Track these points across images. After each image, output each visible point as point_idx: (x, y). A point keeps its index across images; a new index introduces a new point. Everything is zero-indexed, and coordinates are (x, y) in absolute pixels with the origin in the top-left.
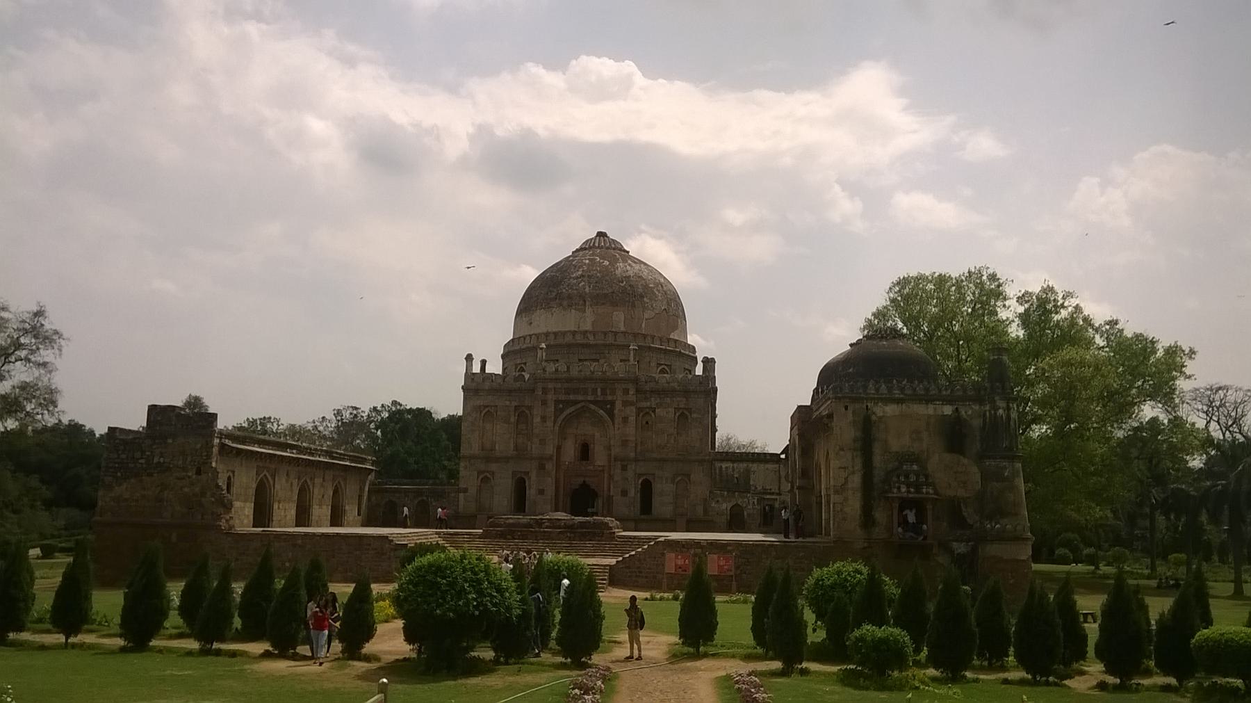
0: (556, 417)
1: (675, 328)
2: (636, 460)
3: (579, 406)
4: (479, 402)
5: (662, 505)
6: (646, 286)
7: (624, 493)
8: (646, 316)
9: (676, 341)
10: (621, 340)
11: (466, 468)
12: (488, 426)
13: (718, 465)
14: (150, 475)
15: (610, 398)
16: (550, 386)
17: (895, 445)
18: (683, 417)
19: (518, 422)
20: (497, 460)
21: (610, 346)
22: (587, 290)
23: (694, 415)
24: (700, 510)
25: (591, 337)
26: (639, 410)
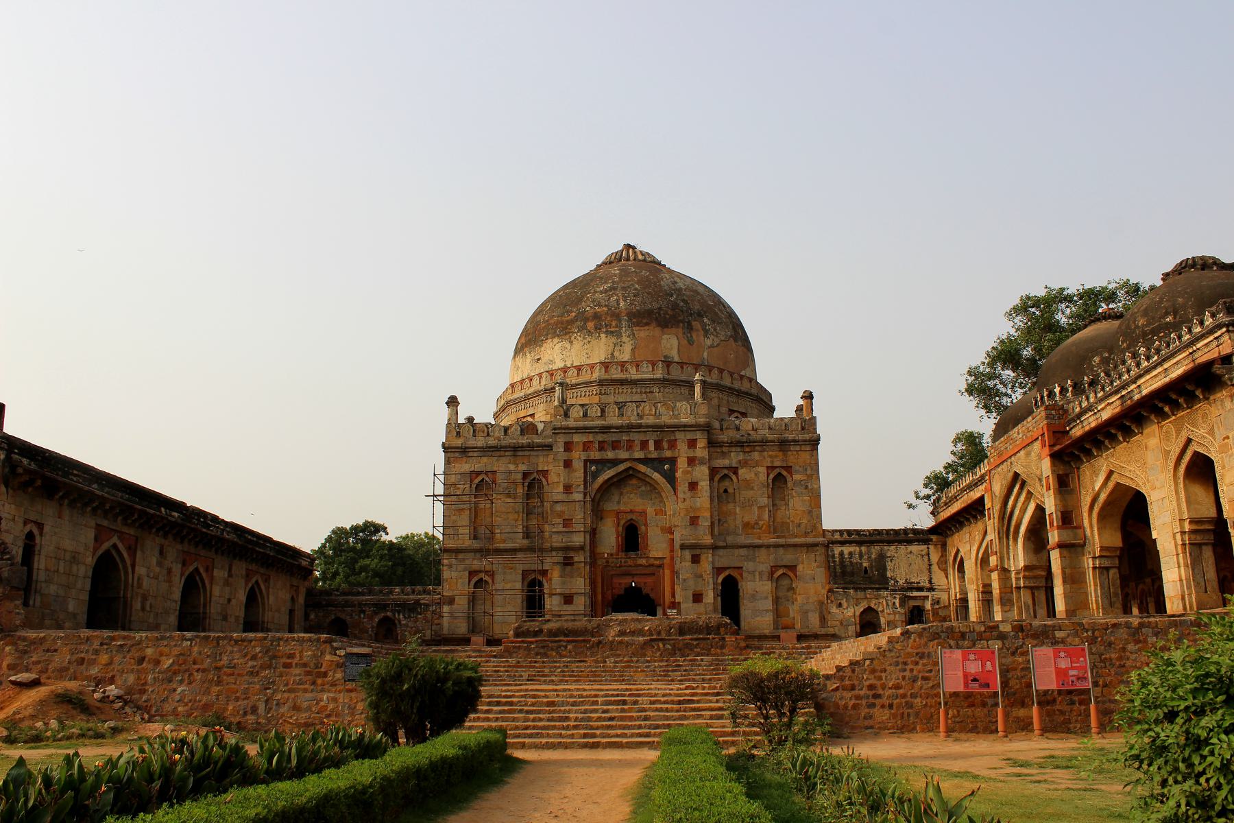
2: (715, 548)
3: (622, 467)
4: (466, 467)
5: (757, 613)
7: (697, 598)
8: (708, 342)
9: (752, 380)
11: (450, 566)
12: (483, 504)
13: (837, 550)
15: (668, 454)
16: (577, 438)
18: (779, 481)
19: (528, 496)
22: (622, 304)
23: (797, 477)
24: (814, 620)
25: (633, 371)
26: (713, 471)
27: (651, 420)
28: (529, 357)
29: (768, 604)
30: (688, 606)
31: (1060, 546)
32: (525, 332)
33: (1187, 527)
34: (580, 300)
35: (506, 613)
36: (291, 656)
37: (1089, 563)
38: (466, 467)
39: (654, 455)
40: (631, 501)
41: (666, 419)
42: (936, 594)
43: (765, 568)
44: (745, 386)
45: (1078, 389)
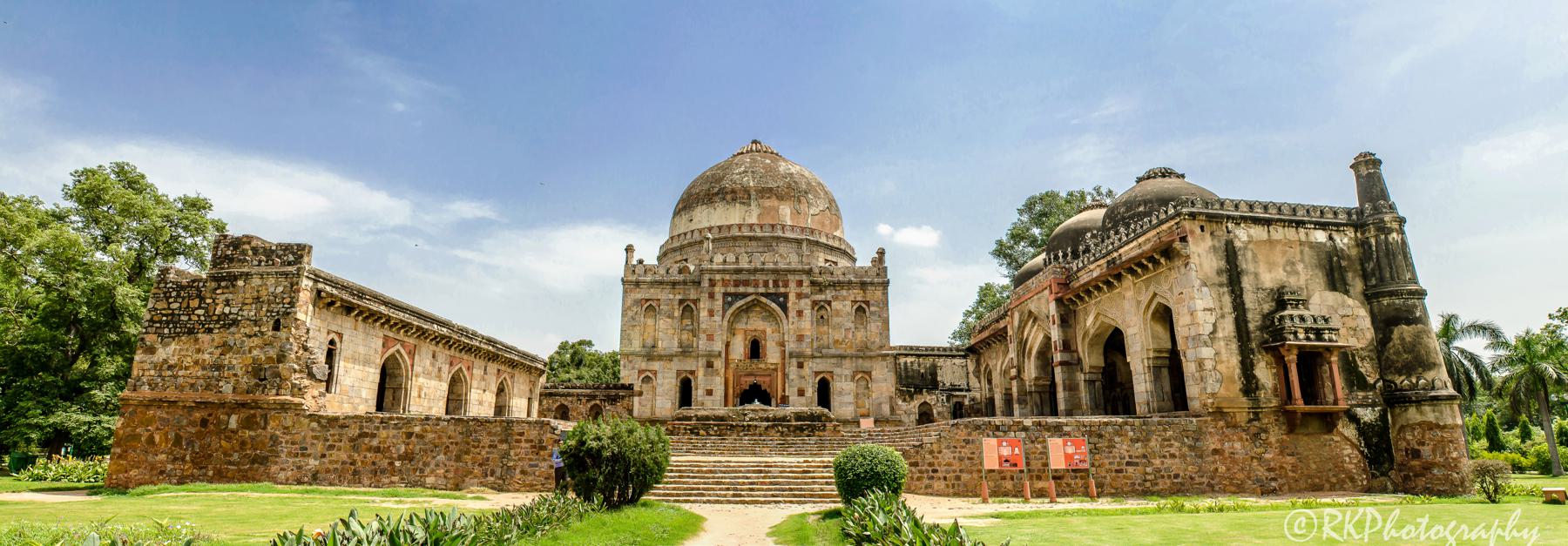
0: (724, 311)
1: (837, 228)
4: (639, 296)
6: (809, 184)
7: (801, 393)
10: (789, 235)
12: (650, 322)
13: (902, 360)
14: (210, 331)
15: (782, 290)
16: (718, 277)
17: (1269, 279)
19: (682, 317)
20: (660, 358)
21: (778, 238)
24: (886, 409)
26: (815, 303)
27: (771, 266)
28: (685, 217)
29: (850, 398)
30: (793, 398)
31: (1062, 363)
32: (682, 200)
33: (1152, 355)
34: (722, 179)
35: (663, 401)
36: (522, 434)
37: (1081, 377)
38: (639, 295)
39: (772, 290)
40: (756, 323)
41: (782, 266)
42: (972, 394)
43: (848, 372)
44: (836, 244)
45: (1076, 255)
